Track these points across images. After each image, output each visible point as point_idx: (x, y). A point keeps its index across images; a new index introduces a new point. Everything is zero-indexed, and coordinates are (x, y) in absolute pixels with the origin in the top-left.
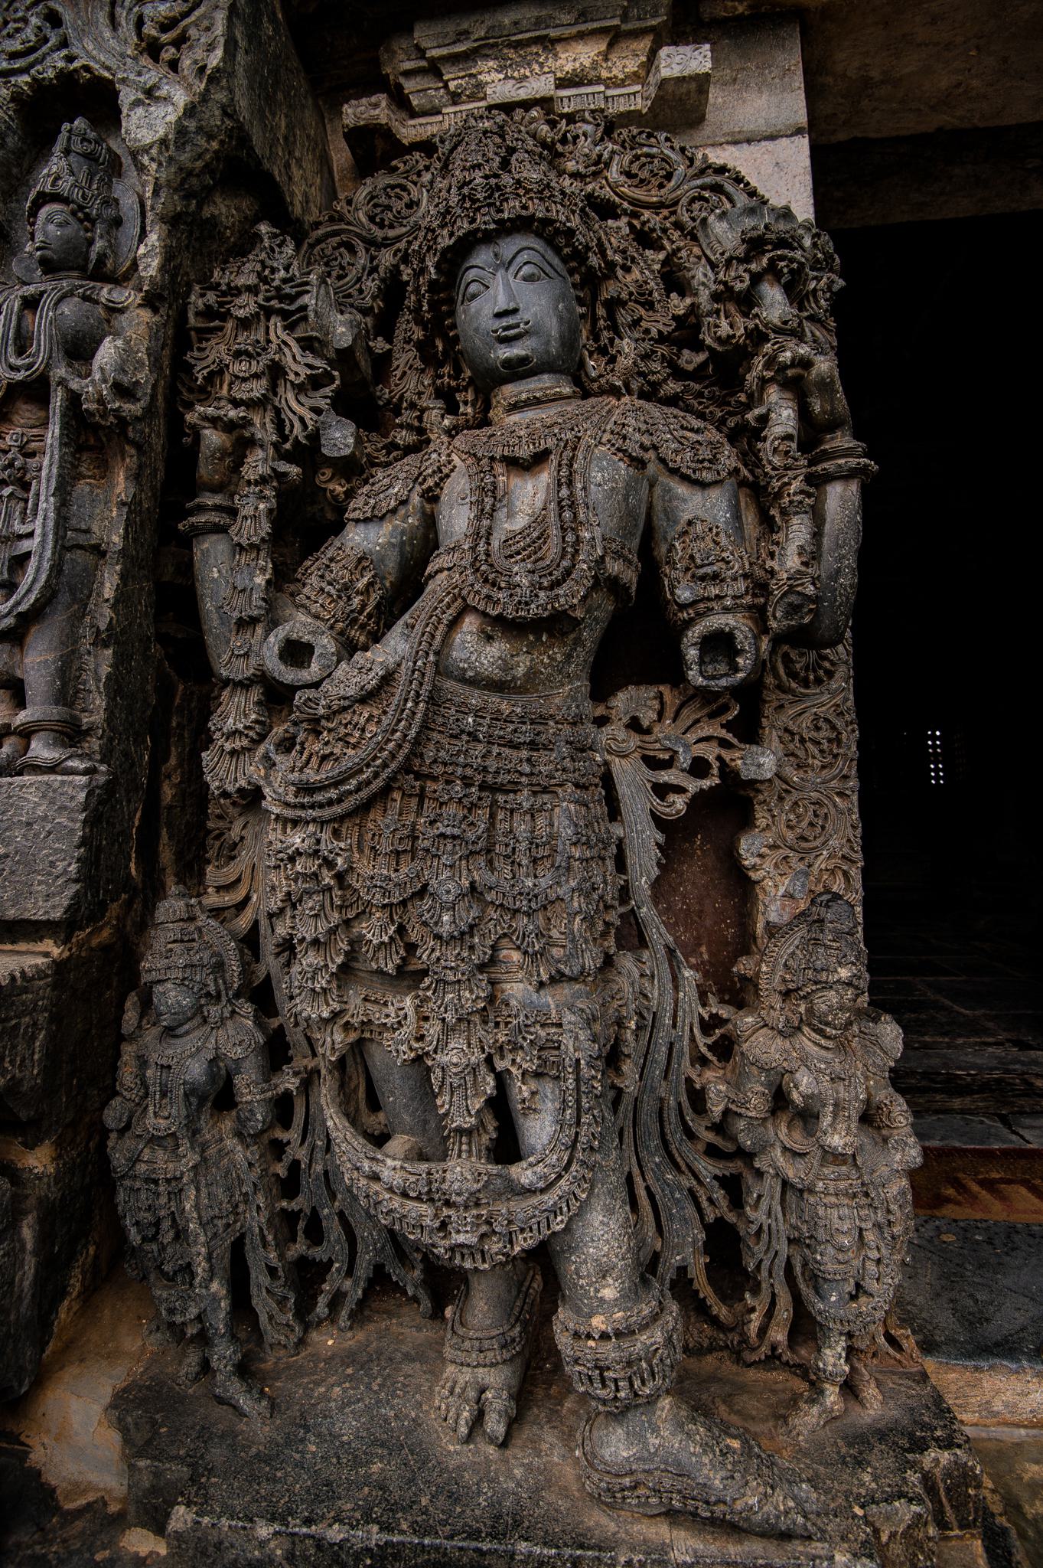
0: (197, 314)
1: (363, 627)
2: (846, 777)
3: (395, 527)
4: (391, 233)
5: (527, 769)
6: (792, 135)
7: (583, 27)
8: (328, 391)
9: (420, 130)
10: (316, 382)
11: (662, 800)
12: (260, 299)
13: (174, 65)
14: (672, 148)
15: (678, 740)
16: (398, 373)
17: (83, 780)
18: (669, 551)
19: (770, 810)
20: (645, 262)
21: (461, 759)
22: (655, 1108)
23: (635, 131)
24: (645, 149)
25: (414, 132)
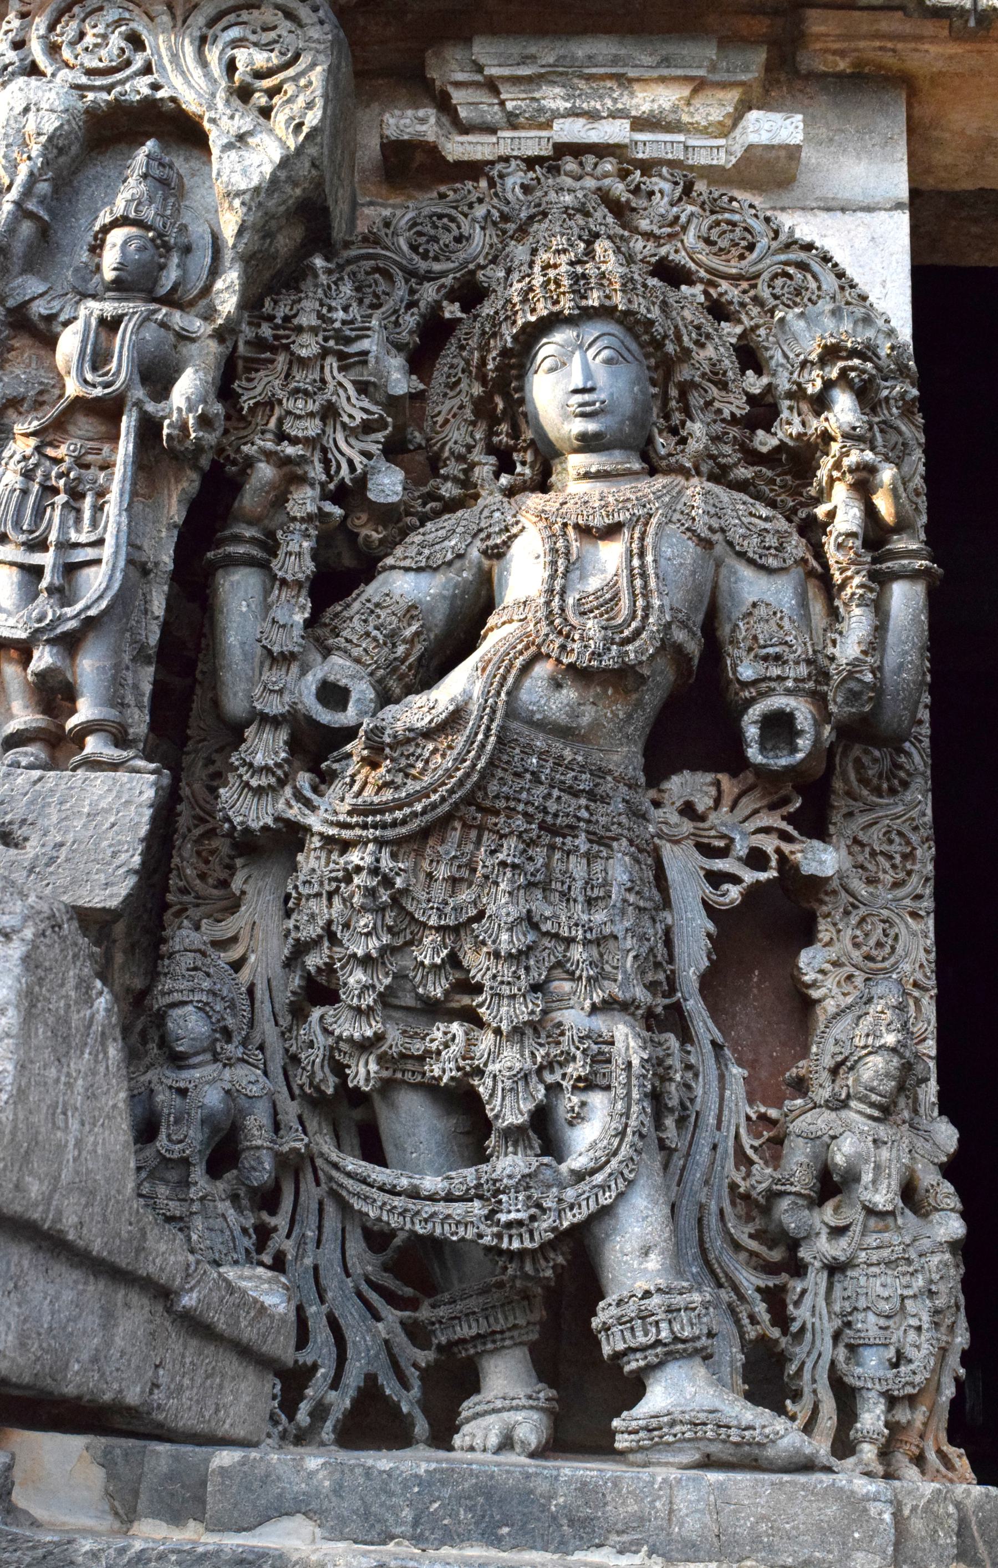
0: (247, 343)
1: (401, 678)
2: (919, 897)
3: (449, 580)
4: (437, 267)
5: (584, 814)
6: (890, 209)
7: (665, 72)
8: (380, 436)
9: (469, 148)
10: (367, 428)
11: (716, 888)
12: (320, 339)
13: (266, 112)
14: (756, 216)
15: (734, 827)
16: (440, 419)
17: (152, 778)
18: (733, 631)
19: (835, 925)
20: (720, 337)
21: (524, 795)
22: (695, 1214)
23: (716, 195)
24: (727, 216)
25: (461, 149)
